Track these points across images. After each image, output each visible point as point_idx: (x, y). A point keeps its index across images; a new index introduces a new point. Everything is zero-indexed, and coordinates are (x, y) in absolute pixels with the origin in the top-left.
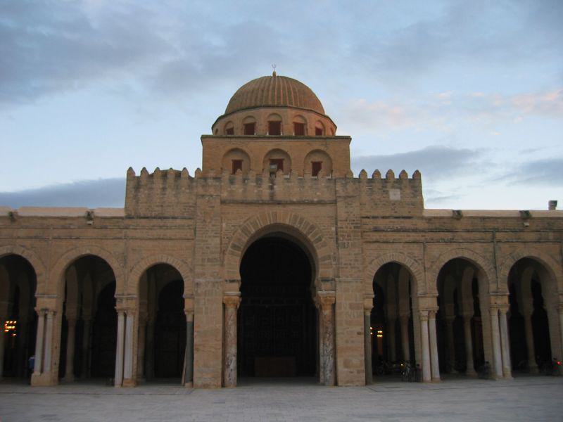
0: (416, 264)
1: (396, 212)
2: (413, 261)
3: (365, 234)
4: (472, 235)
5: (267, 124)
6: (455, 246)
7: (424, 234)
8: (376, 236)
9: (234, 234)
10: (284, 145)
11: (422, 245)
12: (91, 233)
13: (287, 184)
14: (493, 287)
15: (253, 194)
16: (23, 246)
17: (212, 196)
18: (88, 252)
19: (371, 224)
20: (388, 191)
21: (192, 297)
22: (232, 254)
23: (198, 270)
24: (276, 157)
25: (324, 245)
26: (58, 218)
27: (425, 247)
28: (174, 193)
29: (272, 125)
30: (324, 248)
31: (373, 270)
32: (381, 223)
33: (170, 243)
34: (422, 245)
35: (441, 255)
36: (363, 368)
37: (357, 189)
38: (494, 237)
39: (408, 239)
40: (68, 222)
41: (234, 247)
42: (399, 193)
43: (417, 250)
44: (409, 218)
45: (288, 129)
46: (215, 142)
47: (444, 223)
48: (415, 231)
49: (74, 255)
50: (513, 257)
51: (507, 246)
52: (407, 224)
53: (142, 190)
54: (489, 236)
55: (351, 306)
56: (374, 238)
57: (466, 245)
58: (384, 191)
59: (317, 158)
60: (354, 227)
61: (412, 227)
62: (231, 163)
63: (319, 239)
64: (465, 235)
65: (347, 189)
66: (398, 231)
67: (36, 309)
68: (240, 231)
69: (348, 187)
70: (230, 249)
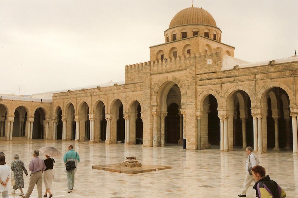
0: (217, 95)
1: (209, 70)
2: (216, 93)
3: (197, 82)
4: (243, 78)
5: (172, 36)
6: (235, 84)
7: (221, 79)
8: (201, 82)
9: (155, 87)
10: (175, 44)
11: (220, 85)
12: (116, 91)
13: (171, 63)
14: (253, 104)
15: (160, 71)
16: (102, 98)
17: (147, 73)
18: (116, 98)
19: (200, 77)
20: (207, 60)
21: (142, 113)
22: (154, 95)
23: (144, 102)
24: (175, 51)
25: (183, 89)
26: (109, 87)
27: (221, 85)
28: (137, 73)
29: (193, 29)
30: (183, 90)
31: (201, 98)
32: (204, 77)
33: (137, 93)
34: (220, 85)
35: (228, 89)
36: (195, 142)
37: (194, 61)
38: (255, 78)
39: (214, 83)
40: (111, 88)
41: (155, 92)
42: (211, 61)
43: (218, 87)
44: (215, 72)
45: (179, 36)
46: (153, 49)
47: (230, 73)
48: (216, 78)
49: (113, 99)
50: (264, 88)
51: (261, 81)
52: (214, 75)
53: (129, 73)
54: (252, 77)
55: (191, 116)
56: (201, 84)
57: (240, 83)
58: (205, 61)
59: (188, 48)
60: (193, 80)
61: (217, 77)
62: (160, 56)
63: (181, 86)
64: (240, 78)
65: (191, 62)
66: (211, 79)
67: (105, 118)
68: (156, 86)
69: (191, 61)
70: (153, 93)
